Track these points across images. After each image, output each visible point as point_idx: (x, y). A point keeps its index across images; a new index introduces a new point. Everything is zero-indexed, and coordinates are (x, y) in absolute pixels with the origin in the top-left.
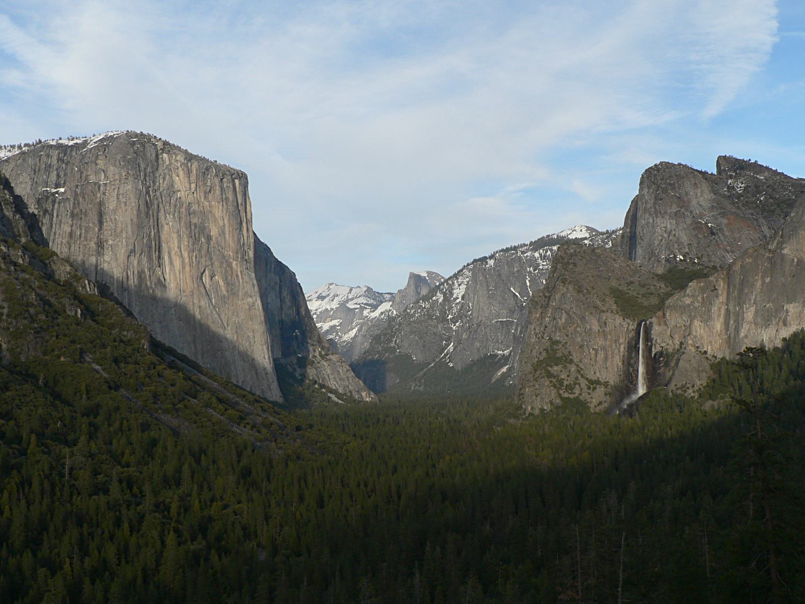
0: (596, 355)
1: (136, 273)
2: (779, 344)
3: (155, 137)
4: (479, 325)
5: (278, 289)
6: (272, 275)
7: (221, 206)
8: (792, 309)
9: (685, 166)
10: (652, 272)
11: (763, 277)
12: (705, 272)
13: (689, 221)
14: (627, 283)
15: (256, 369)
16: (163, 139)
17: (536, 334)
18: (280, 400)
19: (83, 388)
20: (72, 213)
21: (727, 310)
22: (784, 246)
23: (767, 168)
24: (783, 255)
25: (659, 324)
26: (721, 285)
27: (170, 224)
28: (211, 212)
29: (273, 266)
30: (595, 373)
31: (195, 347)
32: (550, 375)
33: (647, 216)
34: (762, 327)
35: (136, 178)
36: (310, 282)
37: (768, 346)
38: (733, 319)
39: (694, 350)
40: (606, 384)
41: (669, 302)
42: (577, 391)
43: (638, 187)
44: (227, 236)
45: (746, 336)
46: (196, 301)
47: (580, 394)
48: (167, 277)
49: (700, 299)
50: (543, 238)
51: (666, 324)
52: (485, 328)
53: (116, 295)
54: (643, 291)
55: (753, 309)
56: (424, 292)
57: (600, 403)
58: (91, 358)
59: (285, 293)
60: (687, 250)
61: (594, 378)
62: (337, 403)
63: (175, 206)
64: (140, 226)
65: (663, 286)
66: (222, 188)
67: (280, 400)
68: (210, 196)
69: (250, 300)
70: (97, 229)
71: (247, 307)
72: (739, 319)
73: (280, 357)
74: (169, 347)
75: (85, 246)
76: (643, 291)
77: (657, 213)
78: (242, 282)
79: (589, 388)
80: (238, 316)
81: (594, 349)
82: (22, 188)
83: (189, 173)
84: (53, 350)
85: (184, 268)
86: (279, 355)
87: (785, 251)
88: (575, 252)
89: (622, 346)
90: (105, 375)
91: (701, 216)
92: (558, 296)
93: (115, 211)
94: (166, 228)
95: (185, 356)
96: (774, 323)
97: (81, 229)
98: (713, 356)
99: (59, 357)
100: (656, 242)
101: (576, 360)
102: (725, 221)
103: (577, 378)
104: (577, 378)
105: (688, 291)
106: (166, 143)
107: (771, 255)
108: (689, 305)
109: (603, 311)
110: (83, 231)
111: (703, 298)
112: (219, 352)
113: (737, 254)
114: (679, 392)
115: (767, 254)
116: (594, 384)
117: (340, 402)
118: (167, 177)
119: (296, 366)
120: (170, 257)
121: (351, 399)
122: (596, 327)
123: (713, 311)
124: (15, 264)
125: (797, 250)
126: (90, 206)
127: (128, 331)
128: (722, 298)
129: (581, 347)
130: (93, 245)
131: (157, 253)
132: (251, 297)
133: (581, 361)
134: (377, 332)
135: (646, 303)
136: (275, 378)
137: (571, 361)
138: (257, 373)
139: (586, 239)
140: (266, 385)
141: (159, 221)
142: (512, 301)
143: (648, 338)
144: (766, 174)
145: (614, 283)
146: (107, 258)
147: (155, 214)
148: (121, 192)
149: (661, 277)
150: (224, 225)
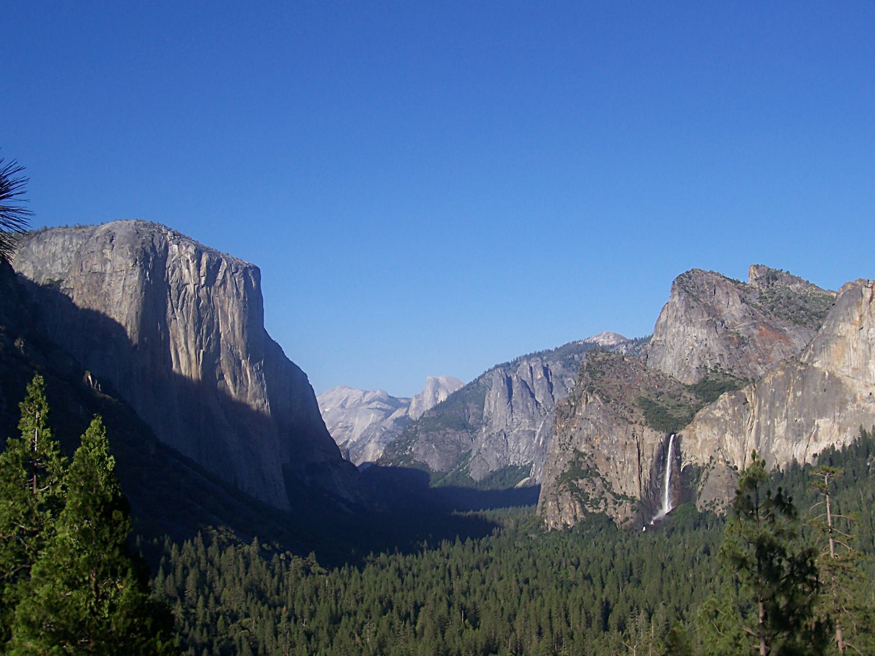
0: (623, 468)
2: (809, 460)
7: (231, 302)
8: (823, 423)
9: (718, 274)
12: (737, 384)
13: (720, 330)
17: (561, 446)
21: (758, 424)
22: (816, 359)
23: (800, 280)
24: (814, 368)
25: (689, 437)
33: (678, 324)
34: (793, 442)
35: (144, 268)
37: (800, 462)
39: (723, 464)
40: (633, 499)
42: (602, 506)
44: (237, 333)
45: (777, 452)
47: (606, 509)
49: (730, 411)
51: (696, 438)
54: (673, 402)
55: (784, 423)
56: (442, 397)
57: (627, 519)
60: (718, 361)
61: (621, 493)
63: (184, 299)
65: (693, 397)
72: (770, 431)
76: (673, 402)
79: (616, 503)
81: (620, 462)
83: (198, 266)
85: (190, 365)
87: (816, 365)
91: (733, 325)
92: (584, 406)
93: (120, 303)
96: (805, 437)
100: (687, 352)
101: (602, 474)
102: (756, 332)
104: (603, 493)
105: (720, 403)
107: (803, 368)
108: (718, 419)
109: (632, 423)
111: (734, 410)
115: (799, 367)
116: (619, 498)
125: (829, 364)
126: (94, 297)
129: (608, 459)
133: (607, 475)
134: (392, 439)
137: (598, 475)
139: (612, 346)
143: (677, 452)
144: (798, 285)
145: (644, 394)
148: (127, 283)
149: (690, 389)
150: (234, 322)
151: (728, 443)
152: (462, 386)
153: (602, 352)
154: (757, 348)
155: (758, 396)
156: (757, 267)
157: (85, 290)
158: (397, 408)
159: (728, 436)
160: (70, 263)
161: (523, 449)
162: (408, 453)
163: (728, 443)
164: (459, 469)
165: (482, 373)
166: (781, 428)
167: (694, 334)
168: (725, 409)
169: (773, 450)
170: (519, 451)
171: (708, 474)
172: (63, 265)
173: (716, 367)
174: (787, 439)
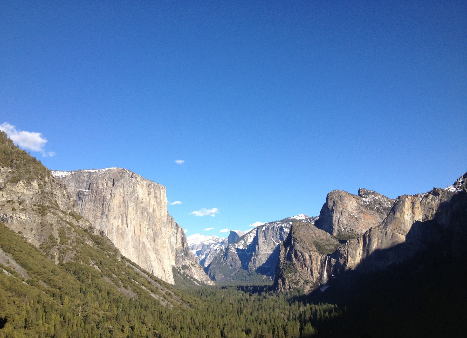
11: (378, 240)
12: (354, 236)
13: (347, 215)
18: (173, 283)
20: (91, 200)
31: (139, 259)
32: (288, 277)
42: (300, 284)
46: (141, 239)
48: (129, 228)
60: (346, 226)
64: (119, 207)
66: (155, 193)
67: (173, 283)
69: (163, 240)
71: (162, 243)
76: (328, 243)
86: (174, 263)
89: (319, 266)
90: (99, 270)
94: (130, 208)
95: (135, 263)
101: (300, 271)
102: (362, 215)
113: (368, 229)
116: (307, 282)
121: (203, 284)
122: (307, 257)
124: (66, 221)
133: (301, 272)
135: (329, 248)
139: (303, 220)
142: (272, 245)
145: (315, 239)
146: (104, 220)
147: (126, 202)
149: (335, 238)
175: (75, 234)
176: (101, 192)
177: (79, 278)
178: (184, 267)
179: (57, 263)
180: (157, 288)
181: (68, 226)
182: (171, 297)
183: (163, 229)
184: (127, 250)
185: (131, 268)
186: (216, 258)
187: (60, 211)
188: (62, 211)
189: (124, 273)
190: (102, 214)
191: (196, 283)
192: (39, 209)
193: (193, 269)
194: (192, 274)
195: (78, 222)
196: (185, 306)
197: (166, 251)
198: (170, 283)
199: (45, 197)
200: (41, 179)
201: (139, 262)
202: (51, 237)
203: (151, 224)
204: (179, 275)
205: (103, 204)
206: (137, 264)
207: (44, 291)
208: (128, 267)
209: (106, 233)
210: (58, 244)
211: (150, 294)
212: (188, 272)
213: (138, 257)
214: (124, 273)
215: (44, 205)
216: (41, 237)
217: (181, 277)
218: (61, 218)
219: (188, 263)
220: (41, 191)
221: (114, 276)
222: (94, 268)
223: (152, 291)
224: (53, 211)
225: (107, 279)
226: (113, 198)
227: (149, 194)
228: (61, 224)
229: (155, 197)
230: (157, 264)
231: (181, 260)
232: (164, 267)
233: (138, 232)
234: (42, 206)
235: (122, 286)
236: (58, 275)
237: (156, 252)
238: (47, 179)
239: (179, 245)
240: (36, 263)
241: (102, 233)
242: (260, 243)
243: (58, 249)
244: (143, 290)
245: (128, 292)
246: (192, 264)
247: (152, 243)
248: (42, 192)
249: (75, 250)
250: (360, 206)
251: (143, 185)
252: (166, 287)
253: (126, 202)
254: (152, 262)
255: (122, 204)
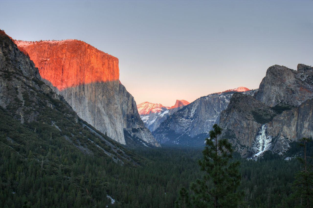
0: (245, 136)
1: (74, 93)
3: (85, 43)
4: (201, 121)
5: (127, 102)
6: (125, 97)
7: (108, 70)
9: (285, 67)
10: (269, 106)
12: (290, 107)
13: (285, 88)
14: (258, 110)
15: (117, 132)
16: (88, 44)
19: (51, 134)
20: (52, 68)
21: (297, 123)
25: (270, 126)
26: (296, 113)
27: (89, 75)
28: (104, 72)
29: (126, 94)
30: (244, 143)
31: (95, 122)
33: (268, 85)
34: (311, 130)
36: (138, 101)
38: (300, 127)
41: (275, 118)
42: (236, 149)
43: (266, 74)
45: (304, 134)
46: (96, 105)
48: (86, 95)
49: (287, 118)
50: (228, 90)
51: (273, 127)
52: (203, 123)
53: (66, 100)
54: (265, 113)
55: (308, 123)
56: (181, 107)
57: (245, 154)
58: (55, 123)
59: (130, 104)
60: (283, 99)
61: (243, 145)
62: (146, 147)
64: (77, 76)
68: (104, 66)
69: (116, 106)
70: (61, 75)
71: (115, 108)
72: (302, 126)
73: (126, 128)
74: (84, 121)
75: (56, 81)
76: (265, 113)
77: (273, 84)
78: (114, 99)
79: (241, 148)
80: (111, 111)
81: (244, 134)
82: (34, 58)
84: (41, 119)
85: (92, 92)
86: (125, 127)
88: (239, 96)
89: (255, 134)
90: (60, 130)
91: (290, 86)
92: (231, 113)
94: (87, 77)
95: (91, 125)
97: (55, 75)
98: (291, 140)
99: (43, 122)
101: (237, 137)
102: (299, 89)
103: (237, 144)
104: (237, 144)
105: (282, 114)
106: (89, 45)
108: (282, 120)
109: (248, 120)
110: (56, 76)
111: (288, 118)
112: (103, 124)
114: (276, 152)
117: (147, 146)
118: (89, 58)
119: (131, 132)
120: (87, 88)
121: (151, 146)
122: (245, 126)
123: (292, 123)
124: (29, 86)
127: (70, 114)
128: (296, 118)
129: (239, 132)
130: (59, 81)
131: (83, 86)
132: (117, 105)
133: (239, 138)
134: (163, 121)
136: (123, 136)
137: (235, 138)
138: (117, 133)
139: (244, 92)
140: (120, 138)
141: (85, 74)
145: (254, 109)
147: (83, 71)
148: (71, 62)
149: (272, 108)
150: (109, 77)
151: (285, 129)
152: (188, 104)
153: (239, 93)
154: (299, 95)
155: (298, 113)
156: (301, 65)
157: (56, 64)
158: (165, 110)
159: (285, 127)
160: (50, 54)
161: (209, 127)
162: (168, 126)
163: (285, 129)
164: (186, 133)
165: (195, 99)
166: (306, 125)
167: (274, 89)
168: (285, 117)
169: (303, 133)
170: (207, 128)
171: (277, 140)
172: (47, 54)
173: (282, 101)
174: (309, 129)
175: (38, 97)
176: (61, 62)
177: (42, 136)
178: (135, 130)
179: (22, 122)
180: (110, 147)
181: (31, 90)
182: (122, 155)
183: (115, 97)
184: (84, 113)
185: (88, 129)
186: (162, 124)
187: (24, 77)
188: (26, 77)
189: (81, 133)
190: (62, 81)
191: (144, 144)
192: (5, 74)
193: (142, 132)
194: (141, 137)
195: (40, 87)
196: (134, 164)
197: (118, 116)
198: (121, 143)
199: (10, 64)
200: (5, 47)
201: (94, 124)
202: (17, 100)
203: (105, 91)
204: (129, 137)
205: (62, 73)
206: (92, 125)
207: (11, 146)
208: (85, 128)
209: (65, 98)
210: (23, 106)
211: (104, 152)
212: (137, 135)
213: (94, 120)
214: (81, 133)
215: (10, 71)
216: (7, 99)
217: (132, 139)
218: (25, 83)
219: (137, 126)
220: (6, 58)
221: (73, 136)
222: (55, 128)
223: (106, 150)
224: (17, 76)
225: (66, 137)
226: (71, 67)
227: (103, 64)
228: (25, 88)
229: (109, 68)
230: (110, 127)
231: (131, 124)
232: (117, 129)
233: (93, 98)
234: (7, 72)
235: (79, 143)
236: (22, 133)
237: (110, 117)
238: (10, 47)
239: (129, 111)
240: (3, 121)
241: (62, 98)
242: (202, 112)
243: (23, 110)
244: (98, 148)
245: (85, 149)
246: (141, 128)
247: (106, 108)
248: (7, 59)
249: (38, 111)
250: (298, 80)
251: (97, 56)
252: (118, 147)
253: (83, 71)
254: (106, 125)
255: (79, 73)
